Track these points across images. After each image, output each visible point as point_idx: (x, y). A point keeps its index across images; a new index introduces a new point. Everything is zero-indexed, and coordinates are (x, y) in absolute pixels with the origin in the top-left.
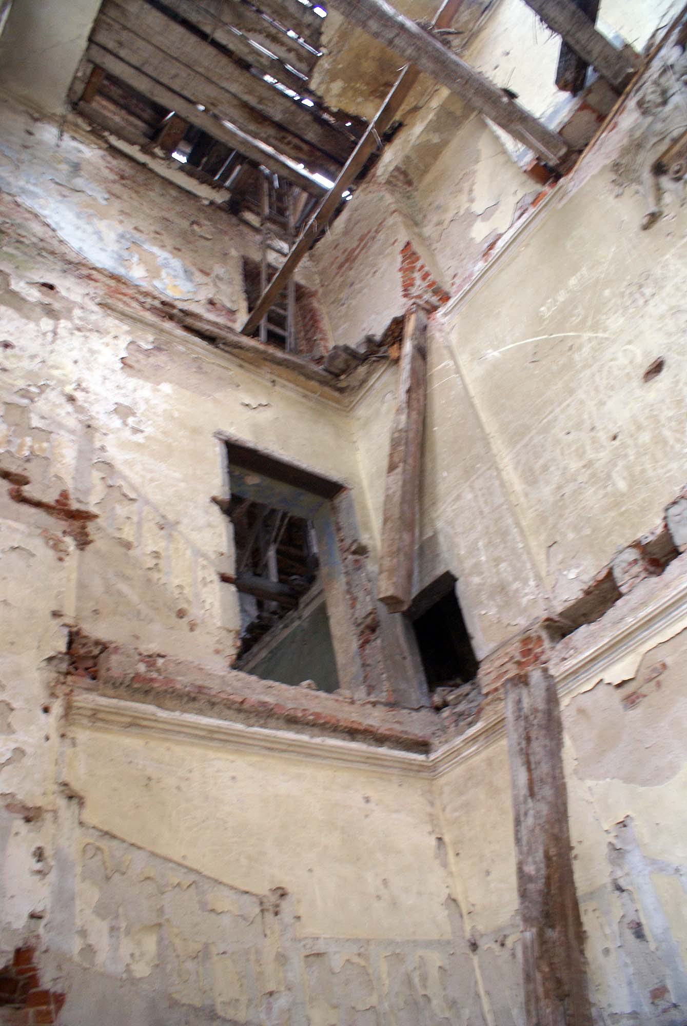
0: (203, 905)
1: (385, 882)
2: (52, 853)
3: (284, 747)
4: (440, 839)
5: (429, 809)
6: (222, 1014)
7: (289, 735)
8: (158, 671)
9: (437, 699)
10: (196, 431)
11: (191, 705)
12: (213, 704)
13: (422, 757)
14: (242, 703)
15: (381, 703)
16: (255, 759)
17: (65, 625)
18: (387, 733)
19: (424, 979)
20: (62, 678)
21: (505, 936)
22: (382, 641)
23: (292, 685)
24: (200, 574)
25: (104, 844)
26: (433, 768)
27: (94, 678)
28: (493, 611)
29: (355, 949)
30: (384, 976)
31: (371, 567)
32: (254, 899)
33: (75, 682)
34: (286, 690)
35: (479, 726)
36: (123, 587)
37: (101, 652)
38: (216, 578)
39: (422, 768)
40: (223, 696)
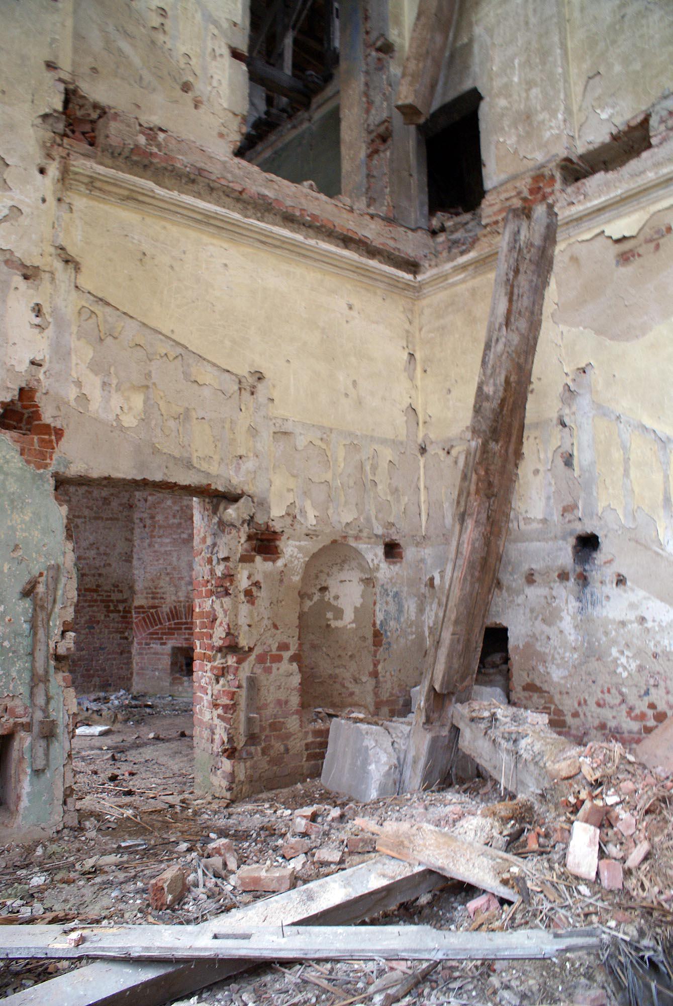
0: (186, 375)
1: (355, 383)
2: (49, 310)
3: (278, 243)
4: (411, 355)
5: (407, 326)
6: (195, 465)
7: (285, 233)
8: (159, 146)
9: (435, 223)
11: (190, 187)
12: (212, 189)
13: (409, 277)
14: (241, 193)
15: (379, 216)
16: (250, 250)
17: (60, 80)
18: (381, 247)
19: (374, 468)
20: (58, 140)
21: (452, 446)
22: (392, 154)
23: (293, 182)
24: (210, 45)
25: (98, 309)
26: (417, 290)
27: (92, 144)
28: (511, 141)
29: (319, 434)
30: (341, 459)
31: (395, 69)
32: (234, 377)
33: (71, 146)
34: (288, 187)
35: (472, 255)
36: (124, 45)
37: (100, 117)
38: (226, 52)
39: (408, 286)
40: (224, 182)
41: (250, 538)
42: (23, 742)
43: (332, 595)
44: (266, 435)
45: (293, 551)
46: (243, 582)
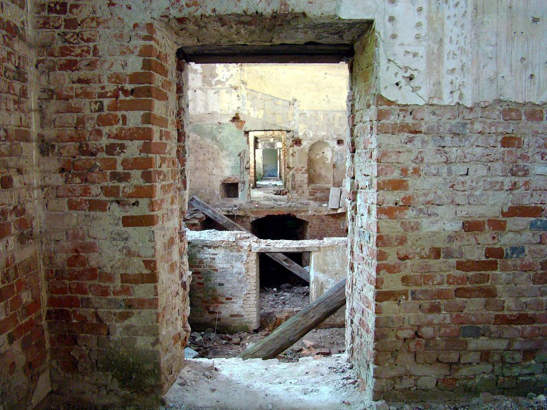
1: (327, 96)
19: (333, 119)
41: (293, 141)
42: (240, 185)
44: (297, 115)
45: (305, 144)
46: (291, 152)
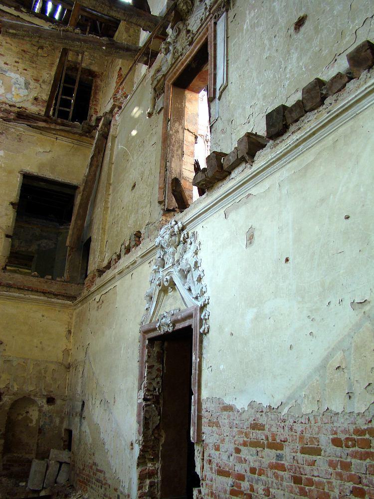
1: (41, 343)
5: (69, 320)
7: (17, 295)
10: (10, 172)
19: (46, 372)
38: (3, 236)
43: (30, 414)
